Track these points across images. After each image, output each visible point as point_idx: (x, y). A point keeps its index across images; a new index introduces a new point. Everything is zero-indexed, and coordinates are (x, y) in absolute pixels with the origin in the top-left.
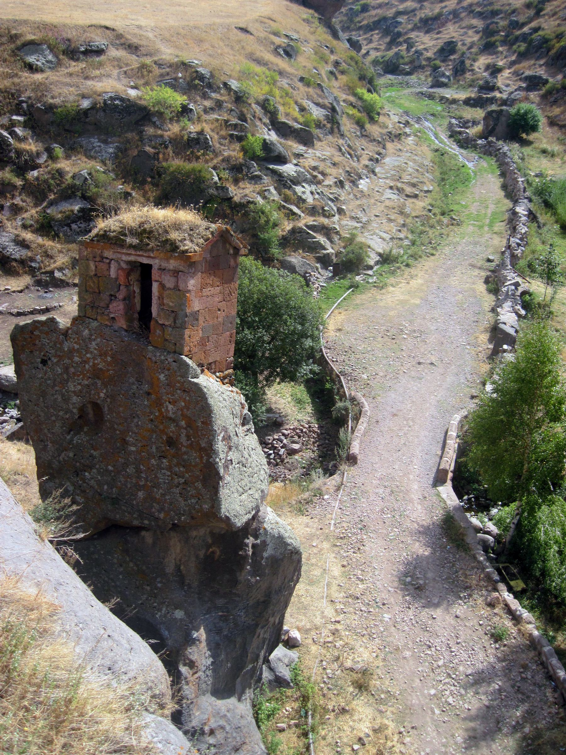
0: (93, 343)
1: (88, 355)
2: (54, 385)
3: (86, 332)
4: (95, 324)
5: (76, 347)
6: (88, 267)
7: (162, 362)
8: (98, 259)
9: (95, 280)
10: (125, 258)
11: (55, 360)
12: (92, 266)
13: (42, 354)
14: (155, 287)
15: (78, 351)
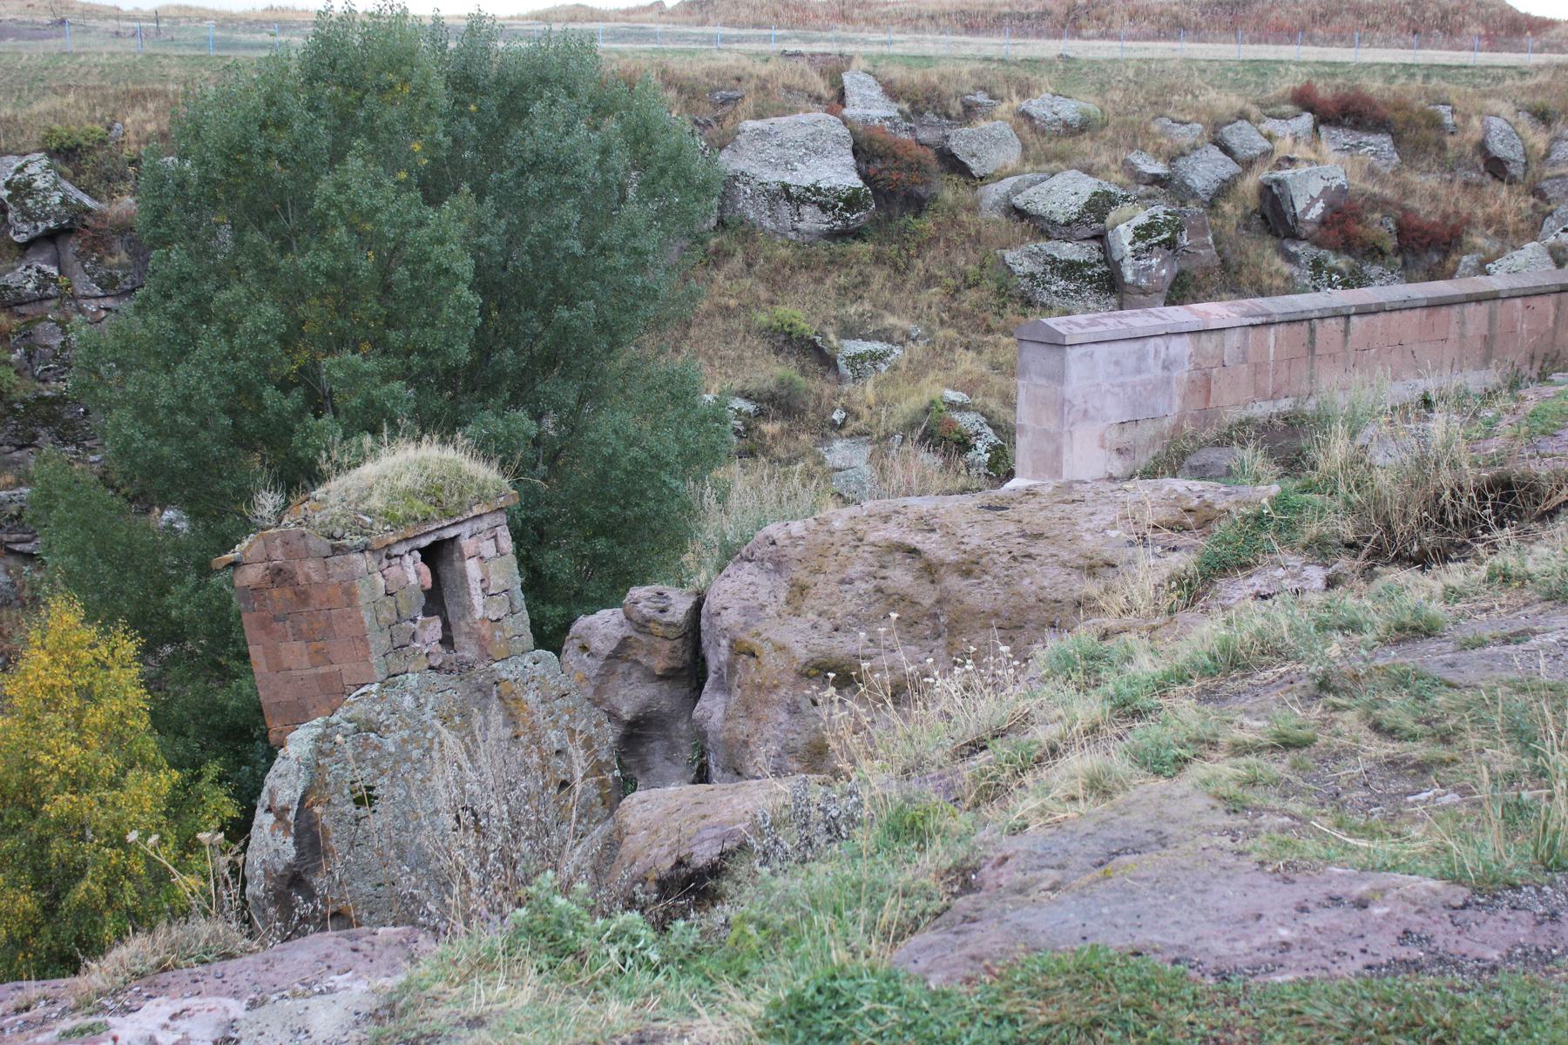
0: (427, 709)
1: (429, 735)
2: (408, 822)
3: (408, 702)
4: (413, 679)
5: (405, 734)
6: (373, 588)
7: (523, 674)
8: (385, 563)
9: (390, 602)
10: (425, 542)
11: (386, 781)
12: (382, 582)
13: (346, 791)
14: (473, 569)
15: (410, 740)
